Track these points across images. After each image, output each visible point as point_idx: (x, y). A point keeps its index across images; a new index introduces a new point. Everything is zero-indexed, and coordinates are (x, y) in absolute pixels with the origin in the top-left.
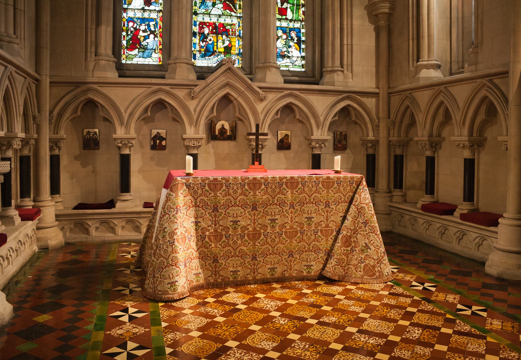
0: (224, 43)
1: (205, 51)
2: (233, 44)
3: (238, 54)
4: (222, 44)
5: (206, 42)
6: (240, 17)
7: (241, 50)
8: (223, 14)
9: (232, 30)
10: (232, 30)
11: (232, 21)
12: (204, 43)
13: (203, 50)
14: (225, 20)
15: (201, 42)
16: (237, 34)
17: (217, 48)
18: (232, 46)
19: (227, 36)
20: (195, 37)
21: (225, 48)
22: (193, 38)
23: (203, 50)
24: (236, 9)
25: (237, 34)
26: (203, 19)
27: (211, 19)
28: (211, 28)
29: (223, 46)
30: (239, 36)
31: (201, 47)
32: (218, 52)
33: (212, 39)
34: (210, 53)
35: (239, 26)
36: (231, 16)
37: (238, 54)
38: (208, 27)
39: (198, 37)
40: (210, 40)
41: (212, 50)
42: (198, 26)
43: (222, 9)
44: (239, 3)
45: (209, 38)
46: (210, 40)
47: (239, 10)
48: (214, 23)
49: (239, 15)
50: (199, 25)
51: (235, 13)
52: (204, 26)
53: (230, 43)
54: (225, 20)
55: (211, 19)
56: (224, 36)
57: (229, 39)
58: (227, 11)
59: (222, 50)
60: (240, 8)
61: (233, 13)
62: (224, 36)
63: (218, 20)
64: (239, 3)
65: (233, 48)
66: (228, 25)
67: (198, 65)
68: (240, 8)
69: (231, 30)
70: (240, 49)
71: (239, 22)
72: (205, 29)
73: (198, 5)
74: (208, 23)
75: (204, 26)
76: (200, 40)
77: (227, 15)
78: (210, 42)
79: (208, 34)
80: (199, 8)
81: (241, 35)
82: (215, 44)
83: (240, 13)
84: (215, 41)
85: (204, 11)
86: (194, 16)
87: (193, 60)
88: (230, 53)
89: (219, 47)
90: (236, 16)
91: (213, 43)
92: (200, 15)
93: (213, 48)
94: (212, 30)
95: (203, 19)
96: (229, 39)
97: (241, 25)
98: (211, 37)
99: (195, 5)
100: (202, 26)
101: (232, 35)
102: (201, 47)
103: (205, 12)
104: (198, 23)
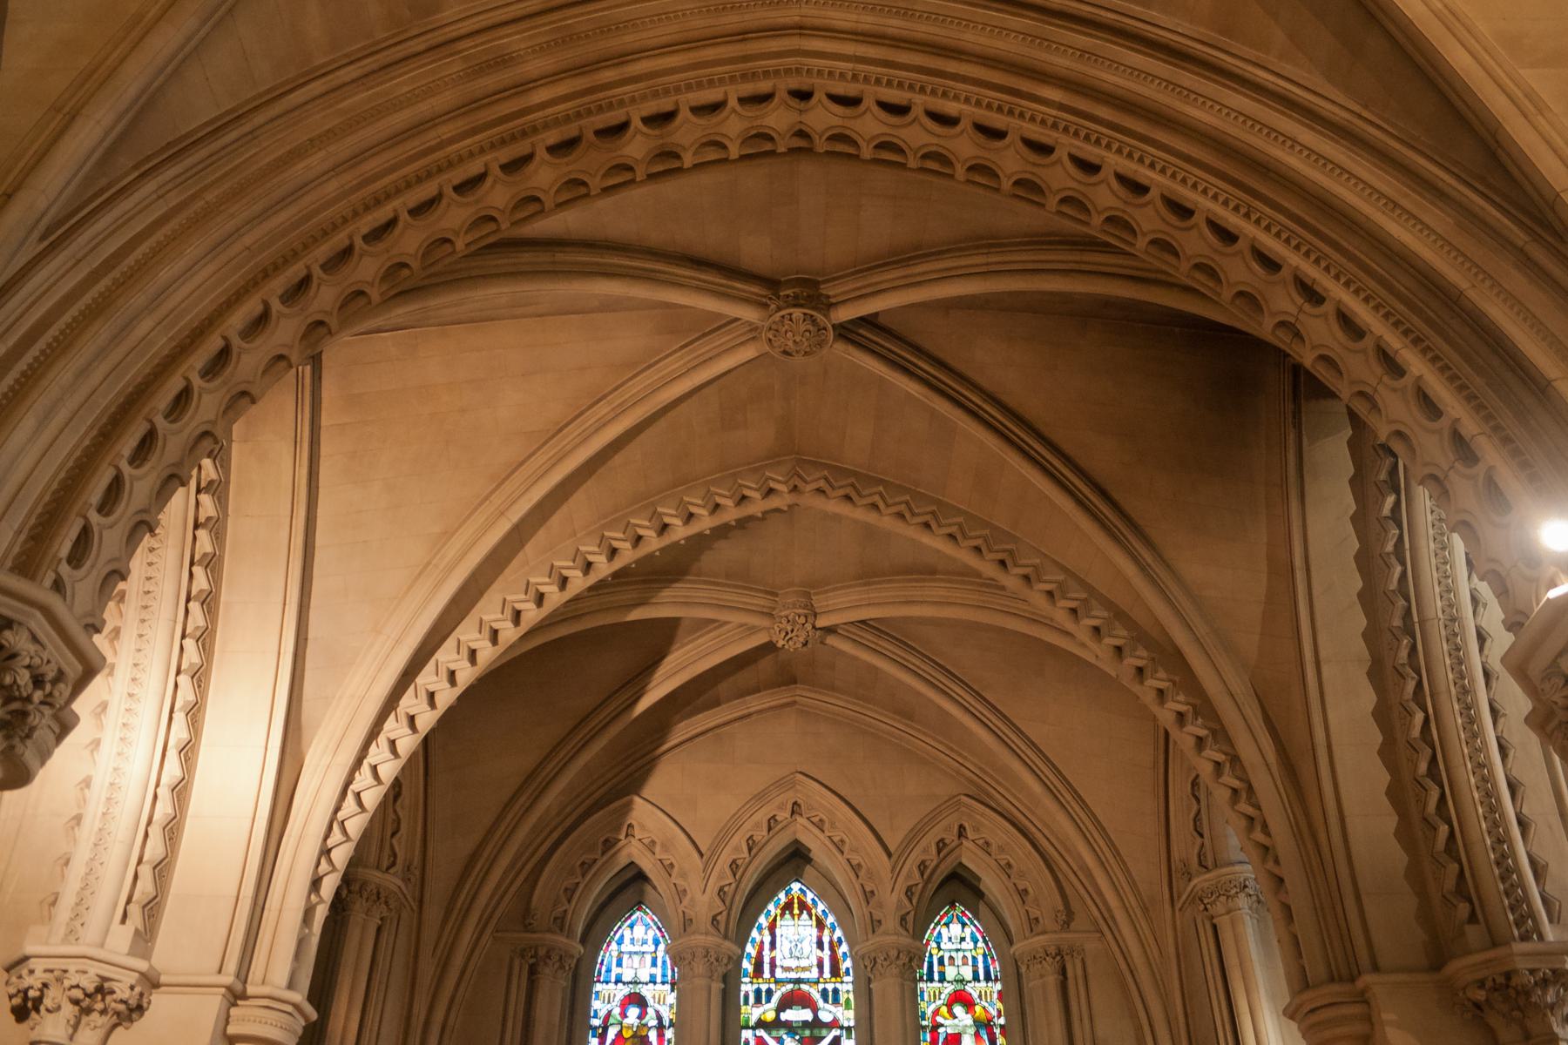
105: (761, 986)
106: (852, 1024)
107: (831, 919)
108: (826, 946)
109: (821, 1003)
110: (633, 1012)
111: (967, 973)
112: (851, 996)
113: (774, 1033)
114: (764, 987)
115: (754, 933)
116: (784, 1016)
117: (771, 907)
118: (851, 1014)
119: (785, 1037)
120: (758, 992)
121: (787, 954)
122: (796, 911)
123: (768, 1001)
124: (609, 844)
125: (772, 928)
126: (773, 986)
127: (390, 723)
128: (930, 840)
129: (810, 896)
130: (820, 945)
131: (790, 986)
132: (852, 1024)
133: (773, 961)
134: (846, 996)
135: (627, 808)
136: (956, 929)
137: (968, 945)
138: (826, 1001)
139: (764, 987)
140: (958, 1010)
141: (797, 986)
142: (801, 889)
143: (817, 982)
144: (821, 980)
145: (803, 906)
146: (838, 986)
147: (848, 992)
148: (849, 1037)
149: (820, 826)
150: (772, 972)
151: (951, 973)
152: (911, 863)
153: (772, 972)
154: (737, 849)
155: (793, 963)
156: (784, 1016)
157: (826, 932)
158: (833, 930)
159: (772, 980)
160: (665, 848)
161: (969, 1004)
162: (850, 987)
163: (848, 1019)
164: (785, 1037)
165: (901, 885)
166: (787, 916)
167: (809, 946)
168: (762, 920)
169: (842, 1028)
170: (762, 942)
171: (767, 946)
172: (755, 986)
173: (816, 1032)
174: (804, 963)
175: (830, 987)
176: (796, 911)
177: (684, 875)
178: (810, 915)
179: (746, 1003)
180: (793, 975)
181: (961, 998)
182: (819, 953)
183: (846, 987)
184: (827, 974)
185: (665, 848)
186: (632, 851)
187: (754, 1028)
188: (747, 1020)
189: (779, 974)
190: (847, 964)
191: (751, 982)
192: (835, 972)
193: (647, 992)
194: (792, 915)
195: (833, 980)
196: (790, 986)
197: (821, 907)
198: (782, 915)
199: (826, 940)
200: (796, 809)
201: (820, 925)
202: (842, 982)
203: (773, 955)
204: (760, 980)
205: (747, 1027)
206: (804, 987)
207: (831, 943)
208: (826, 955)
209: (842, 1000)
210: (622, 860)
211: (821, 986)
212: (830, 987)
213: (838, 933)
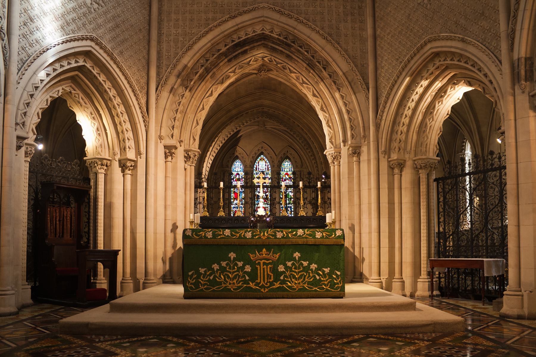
107: (267, 161)
110: (238, 176)
111: (288, 170)
124: (234, 154)
125: (258, 163)
127: (210, 156)
128: (282, 153)
130: (266, 166)
135: (236, 148)
136: (287, 163)
137: (289, 166)
140: (286, 176)
145: (263, 159)
149: (266, 150)
151: (286, 170)
152: (279, 157)
154: (253, 154)
155: (262, 168)
160: (242, 154)
161: (288, 175)
165: (278, 160)
167: (264, 166)
177: (245, 159)
181: (287, 174)
183: (270, 172)
185: (242, 154)
186: (237, 154)
190: (270, 169)
192: (268, 170)
193: (239, 173)
197: (266, 159)
200: (262, 148)
201: (266, 162)
208: (267, 167)
210: (236, 155)
213: (269, 164)
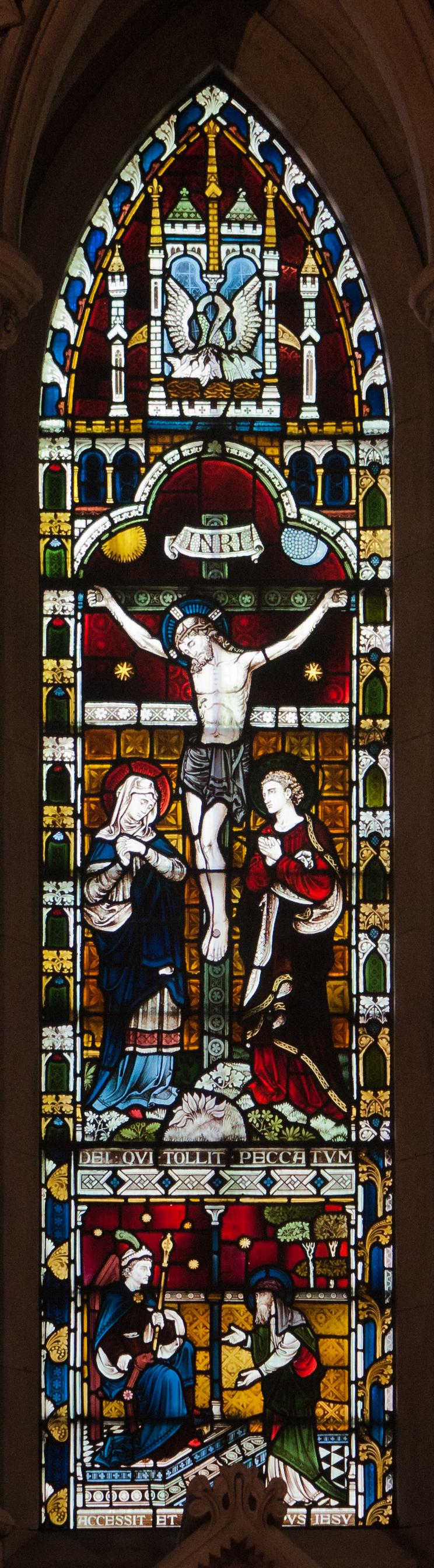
0: (260, 1353)
1: (126, 1421)
2: (329, 1350)
3: (363, 1429)
4: (245, 1358)
5: (138, 1348)
6: (374, 1150)
7: (389, 1393)
8: (255, 1138)
9: (322, 1245)
10: (322, 1245)
11: (319, 1182)
12: (124, 1360)
13: (112, 1409)
14: (268, 1182)
15: (102, 1359)
16: (359, 1271)
17: (217, 1391)
18: (322, 1370)
19: (285, 1298)
20: (61, 1322)
21: (267, 1383)
22: (49, 1328)
23: (112, 1409)
24: (345, 1093)
25: (359, 1271)
26: (116, 1182)
27: (167, 1182)
28: (167, 1245)
29: (253, 1375)
30: (372, 1288)
31: (101, 1390)
32: (226, 1418)
33: (180, 1328)
34: (164, 1433)
35: (370, 1217)
36: (312, 1142)
37: (363, 1429)
38: (150, 1237)
39: (77, 1320)
40: (167, 1334)
41: (176, 1405)
42: (76, 1238)
43: (247, 1102)
44: (366, 1041)
45: (158, 1319)
46: (167, 1334)
47: (367, 1096)
48: (194, 1208)
49: (367, 1133)
50: (86, 1230)
51: (340, 1118)
52: (122, 1235)
53: (309, 1348)
54: (268, 1182)
55: (167, 1182)
56: (263, 1302)
57: (298, 1319)
58: (285, 1108)
59: (252, 1402)
60: (374, 1083)
61: (323, 1125)
62: (263, 1302)
63: (217, 1182)
64: (366, 1041)
65: (330, 1384)
66: (292, 1210)
67: (85, 1521)
68: (374, 1083)
69: (310, 1248)
70: (378, 1388)
71: (370, 1188)
72: (130, 1254)
73: (75, 1084)
74: (148, 1206)
75: (122, 1235)
76: (90, 1335)
77: (282, 1143)
78: (166, 1352)
79: (150, 1290)
80: (87, 1106)
81: (388, 1285)
82: (203, 1360)
83: (375, 1121)
84: (202, 1336)
85: (115, 1120)
86: (50, 1165)
87: (48, 1490)
88: (311, 1421)
89: (227, 1381)
90: (347, 1144)
91: (185, 1357)
92: (94, 1158)
93: (189, 1392)
94: (179, 1257)
95: (116, 1182)
96: (298, 1319)
97: (385, 1205)
98: (171, 1315)
99: (58, 1087)
100: (109, 1233)
101: (322, 1287)
102: (101, 1390)
103: (127, 1133)
104: (77, 1215)
105: (101, 445)
106: (385, 572)
108: (310, 309)
109: (290, 506)
112: (385, 484)
113: (144, 602)
114: (110, 449)
115: (79, 266)
116: (174, 547)
117: (131, 173)
118: (381, 541)
119: (176, 613)
120: (92, 463)
121: (183, 336)
122: (213, 190)
123: (125, 497)
126: (138, 447)
129: (259, 134)
131: (191, 448)
132: (385, 572)
133: (138, 356)
134: (368, 482)
138: (304, 499)
139: (110, 449)
141: (214, 448)
142: (226, 110)
143: (280, 436)
144: (292, 428)
146: (347, 448)
147: (375, 468)
148: (375, 621)
150: (137, 402)
153: (137, 402)
155: (201, 371)
156: (174, 547)
157: (310, 264)
158: (330, 265)
159: (137, 425)
162: (381, 453)
163: (376, 560)
164: (176, 613)
166: (185, 206)
168: (102, 218)
169: (353, 585)
170: (103, 296)
171: (118, 309)
172: (82, 446)
173: (275, 599)
174: (240, 369)
175: (318, 451)
176: (213, 190)
178: (258, 204)
179: (55, 503)
180: (202, 410)
182: (288, 339)
184: (310, 413)
187: (79, 585)
188: (59, 561)
189: (157, 409)
191: (70, 434)
194: (201, 204)
195: (330, 428)
196: (191, 448)
198: (168, 202)
199: (309, 289)
202: (357, 437)
203: (138, 338)
204: (99, 427)
205: (59, 583)
206: (241, 451)
207: (323, 300)
209: (356, 497)
211: (291, 449)
212: (318, 451)
